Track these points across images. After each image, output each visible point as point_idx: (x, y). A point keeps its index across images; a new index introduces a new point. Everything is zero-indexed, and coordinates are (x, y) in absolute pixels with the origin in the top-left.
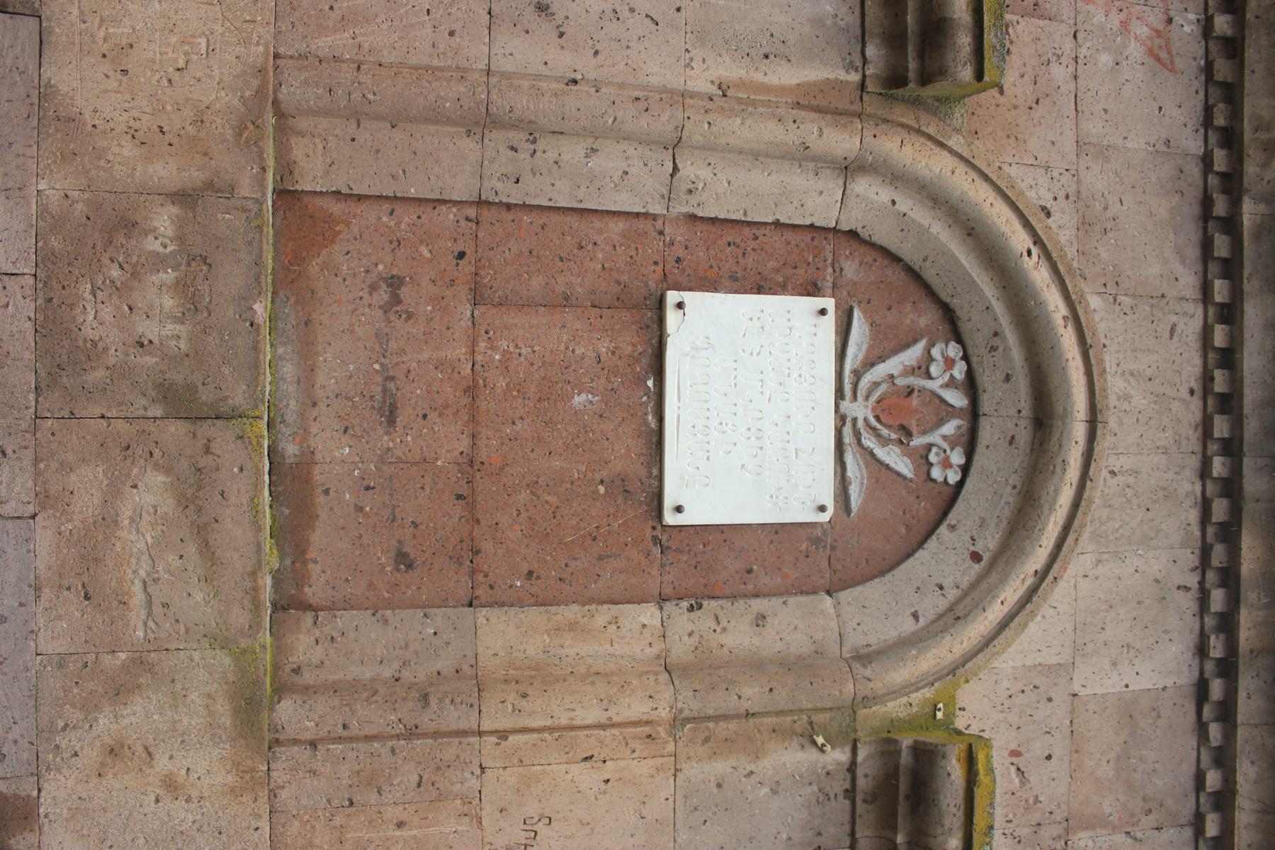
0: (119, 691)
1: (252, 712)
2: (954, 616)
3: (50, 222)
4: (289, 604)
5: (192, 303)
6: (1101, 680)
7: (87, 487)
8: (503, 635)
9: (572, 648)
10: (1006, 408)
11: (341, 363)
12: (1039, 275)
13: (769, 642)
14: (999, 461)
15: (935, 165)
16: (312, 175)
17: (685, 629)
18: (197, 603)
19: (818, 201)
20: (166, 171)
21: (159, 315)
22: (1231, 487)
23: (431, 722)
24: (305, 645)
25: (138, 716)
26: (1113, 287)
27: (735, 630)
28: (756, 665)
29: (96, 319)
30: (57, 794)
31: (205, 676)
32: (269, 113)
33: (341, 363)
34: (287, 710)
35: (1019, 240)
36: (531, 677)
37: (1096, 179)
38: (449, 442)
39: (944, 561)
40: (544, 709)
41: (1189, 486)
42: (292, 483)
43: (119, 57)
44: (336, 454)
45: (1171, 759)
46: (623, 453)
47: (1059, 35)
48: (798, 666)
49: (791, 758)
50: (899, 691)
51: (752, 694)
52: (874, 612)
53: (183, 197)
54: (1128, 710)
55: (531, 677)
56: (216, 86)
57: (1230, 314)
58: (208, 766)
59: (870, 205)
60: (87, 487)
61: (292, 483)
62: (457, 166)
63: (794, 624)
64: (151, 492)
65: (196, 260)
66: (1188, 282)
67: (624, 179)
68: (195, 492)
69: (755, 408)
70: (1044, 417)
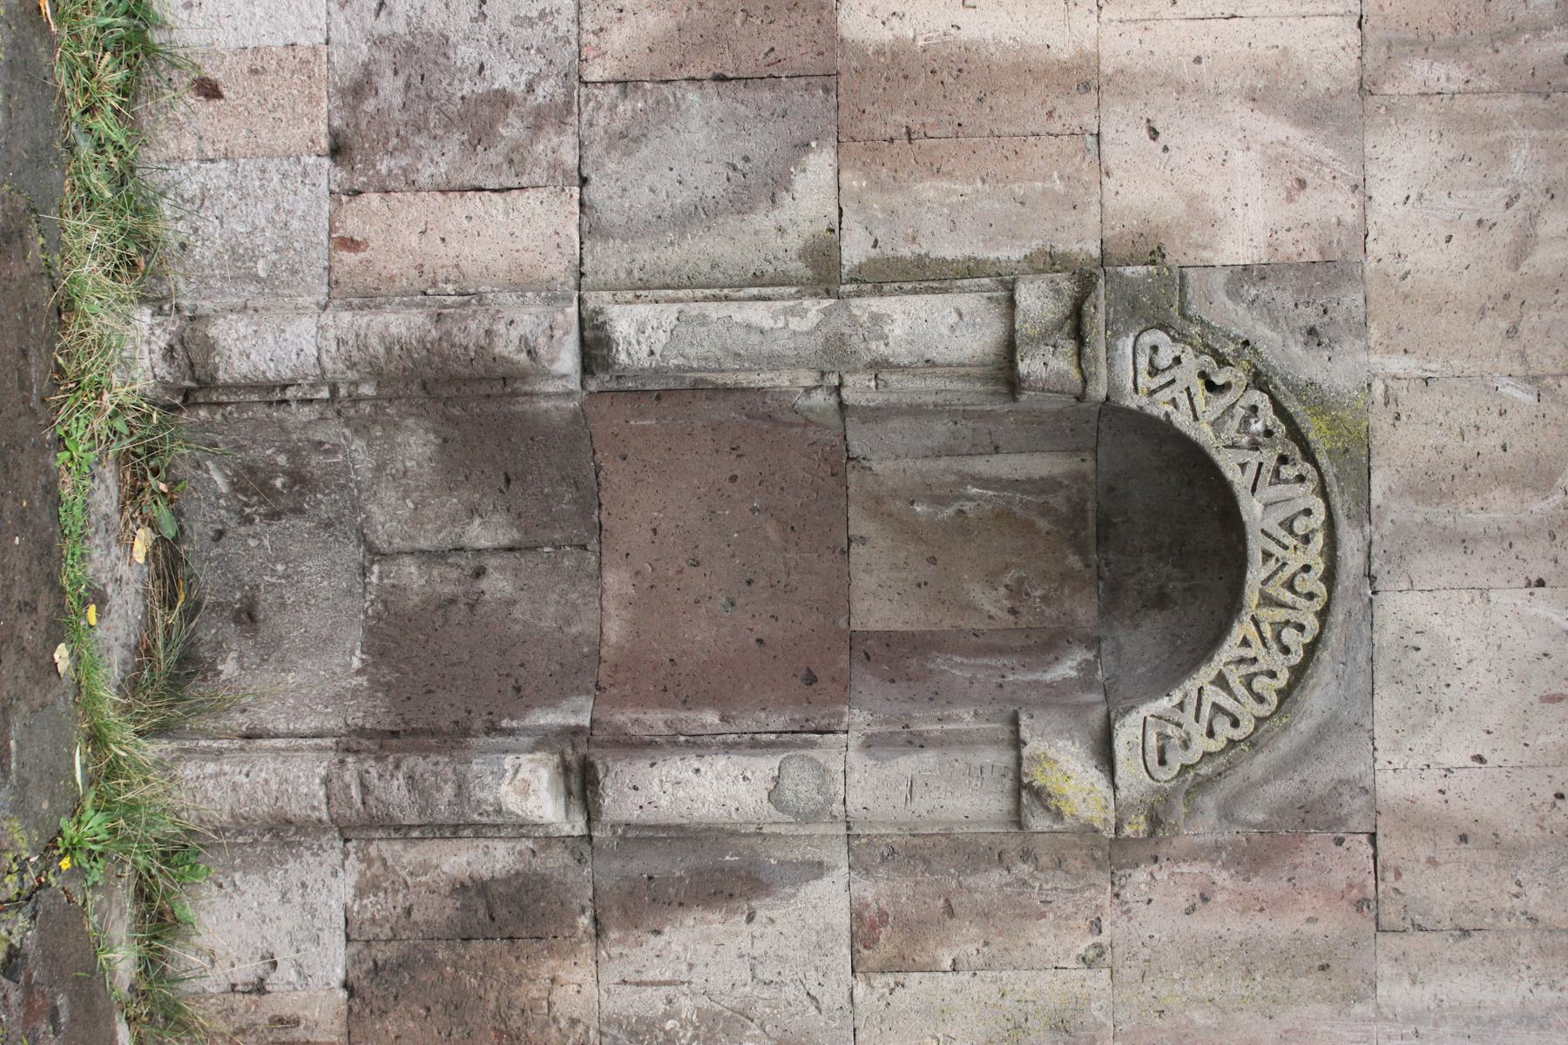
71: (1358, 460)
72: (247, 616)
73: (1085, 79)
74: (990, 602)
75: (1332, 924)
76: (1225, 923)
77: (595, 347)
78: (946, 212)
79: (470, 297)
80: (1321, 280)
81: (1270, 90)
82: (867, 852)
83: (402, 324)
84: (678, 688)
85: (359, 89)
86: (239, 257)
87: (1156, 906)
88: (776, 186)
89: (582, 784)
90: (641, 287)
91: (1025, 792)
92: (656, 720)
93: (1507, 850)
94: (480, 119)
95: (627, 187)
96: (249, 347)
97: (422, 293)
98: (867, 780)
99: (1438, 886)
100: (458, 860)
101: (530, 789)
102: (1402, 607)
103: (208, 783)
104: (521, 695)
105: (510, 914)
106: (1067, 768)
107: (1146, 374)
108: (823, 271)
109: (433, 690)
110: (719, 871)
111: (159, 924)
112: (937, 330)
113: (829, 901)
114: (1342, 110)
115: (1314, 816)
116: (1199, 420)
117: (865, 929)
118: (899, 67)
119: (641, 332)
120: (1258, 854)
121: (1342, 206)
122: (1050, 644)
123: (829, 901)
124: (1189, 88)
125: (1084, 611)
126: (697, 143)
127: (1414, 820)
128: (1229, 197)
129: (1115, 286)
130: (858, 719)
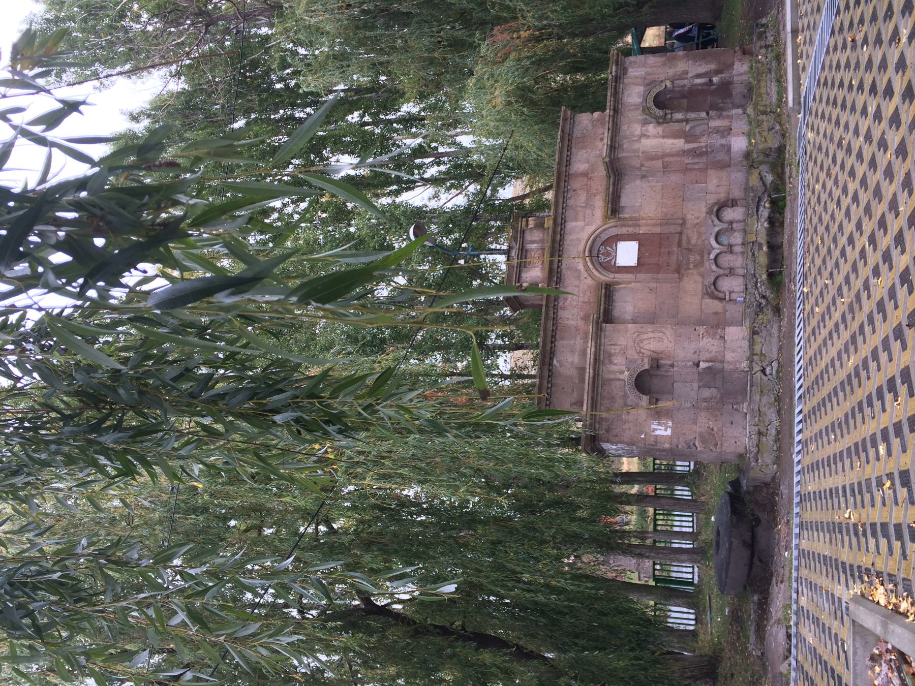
0: (697, 224)
1: (684, 222)
2: (605, 230)
3: (702, 266)
4: (681, 233)
5: (688, 259)
6: (580, 224)
7: (699, 242)
8: (658, 230)
9: (650, 228)
10: (595, 253)
11: (674, 258)
12: (591, 267)
13: (627, 228)
14: (596, 248)
15: (603, 278)
16: (677, 275)
17: (637, 230)
18: (689, 232)
19: (617, 275)
20: (691, 271)
21: (692, 258)
22: (560, 246)
23: (666, 221)
24: (679, 229)
25: (696, 221)
26: (576, 270)
27: (631, 230)
28: (629, 226)
29: (698, 257)
30: (704, 215)
31: (688, 225)
32: (681, 279)
33: (674, 258)
34: (681, 222)
35: (594, 271)
36: (655, 225)
37: (577, 283)
38: (662, 250)
39: (604, 237)
40: (654, 222)
41: (565, 247)
42: (680, 245)
43: (695, 282)
44: (675, 249)
45: (569, 214)
46: (643, 249)
47: (581, 300)
48: (624, 226)
49: (626, 216)
50: (612, 222)
51: (630, 223)
52: (614, 232)
53: (689, 269)
54: (576, 220)
55: (655, 225)
56: (686, 279)
57: (558, 267)
58: (689, 217)
59: (612, 275)
60: (699, 242)
61: (680, 245)
62: (660, 276)
63: (624, 230)
64: (693, 242)
65: (688, 263)
66: (563, 271)
67: (641, 276)
68: (689, 242)
69: (627, 254)
70: (590, 252)
71: (644, 110)
72: (744, 96)
73: (664, 137)
74: (675, 103)
75: (648, 77)
76: (656, 76)
77: (708, 114)
78: (676, 126)
79: (719, 117)
80: (645, 123)
81: (648, 137)
82: (687, 78)
83: (725, 113)
84: (703, 91)
85: (729, 134)
86: (741, 120)
87: (662, 77)
88: (691, 128)
89: (711, 81)
90: (703, 119)
91: (673, 82)
92: (705, 87)
93: (634, 84)
94: (717, 132)
95: (705, 127)
96: (740, 111)
97: (724, 118)
98: (686, 82)
99: (639, 81)
100: (723, 75)
101: (715, 79)
102: (640, 100)
103: (745, 77)
104: (717, 89)
105: (717, 72)
106: (669, 84)
107: (659, 112)
108: (687, 121)
109: (725, 89)
110: (699, 76)
111: (751, 68)
112: (679, 116)
113: (690, 75)
114: (643, 135)
115: (649, 85)
116: (657, 110)
117: (687, 73)
118: (679, 137)
119: (703, 115)
120: (654, 81)
121: (644, 129)
122: (670, 98)
123: (690, 75)
124: (655, 137)
125: (667, 102)
126: (698, 131)
127: (641, 85)
128: (652, 129)
129: (662, 121)
130: (686, 88)
